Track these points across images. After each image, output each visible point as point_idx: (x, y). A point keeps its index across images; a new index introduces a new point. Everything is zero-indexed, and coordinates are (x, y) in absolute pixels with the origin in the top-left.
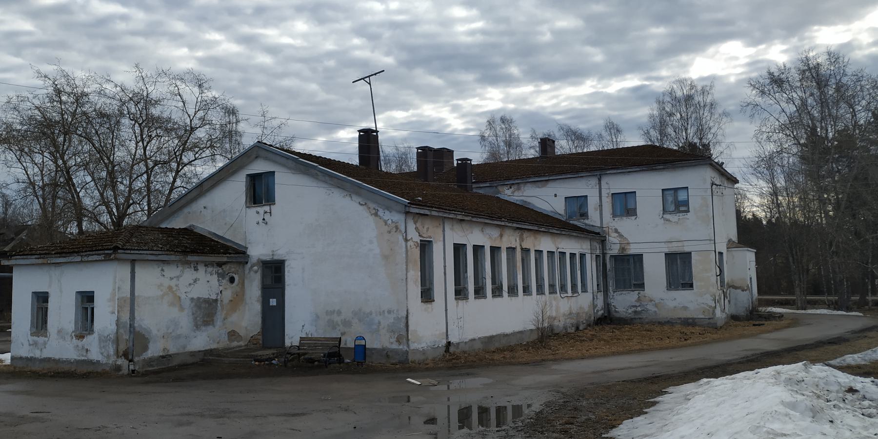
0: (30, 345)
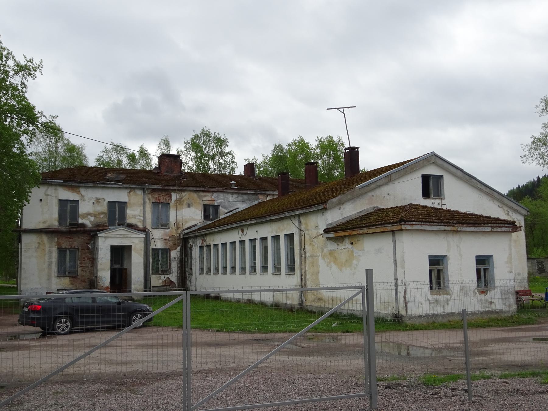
0: (430, 303)
